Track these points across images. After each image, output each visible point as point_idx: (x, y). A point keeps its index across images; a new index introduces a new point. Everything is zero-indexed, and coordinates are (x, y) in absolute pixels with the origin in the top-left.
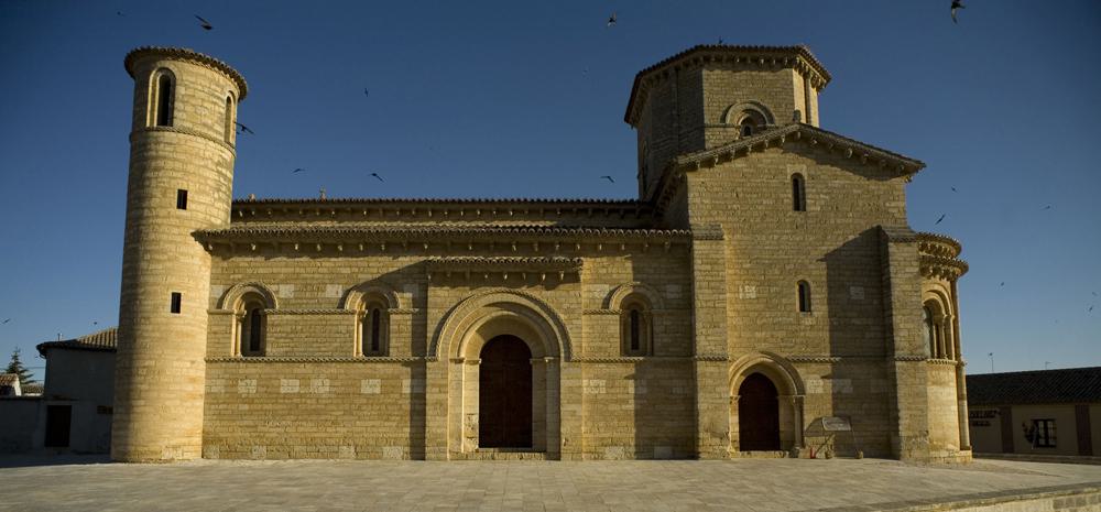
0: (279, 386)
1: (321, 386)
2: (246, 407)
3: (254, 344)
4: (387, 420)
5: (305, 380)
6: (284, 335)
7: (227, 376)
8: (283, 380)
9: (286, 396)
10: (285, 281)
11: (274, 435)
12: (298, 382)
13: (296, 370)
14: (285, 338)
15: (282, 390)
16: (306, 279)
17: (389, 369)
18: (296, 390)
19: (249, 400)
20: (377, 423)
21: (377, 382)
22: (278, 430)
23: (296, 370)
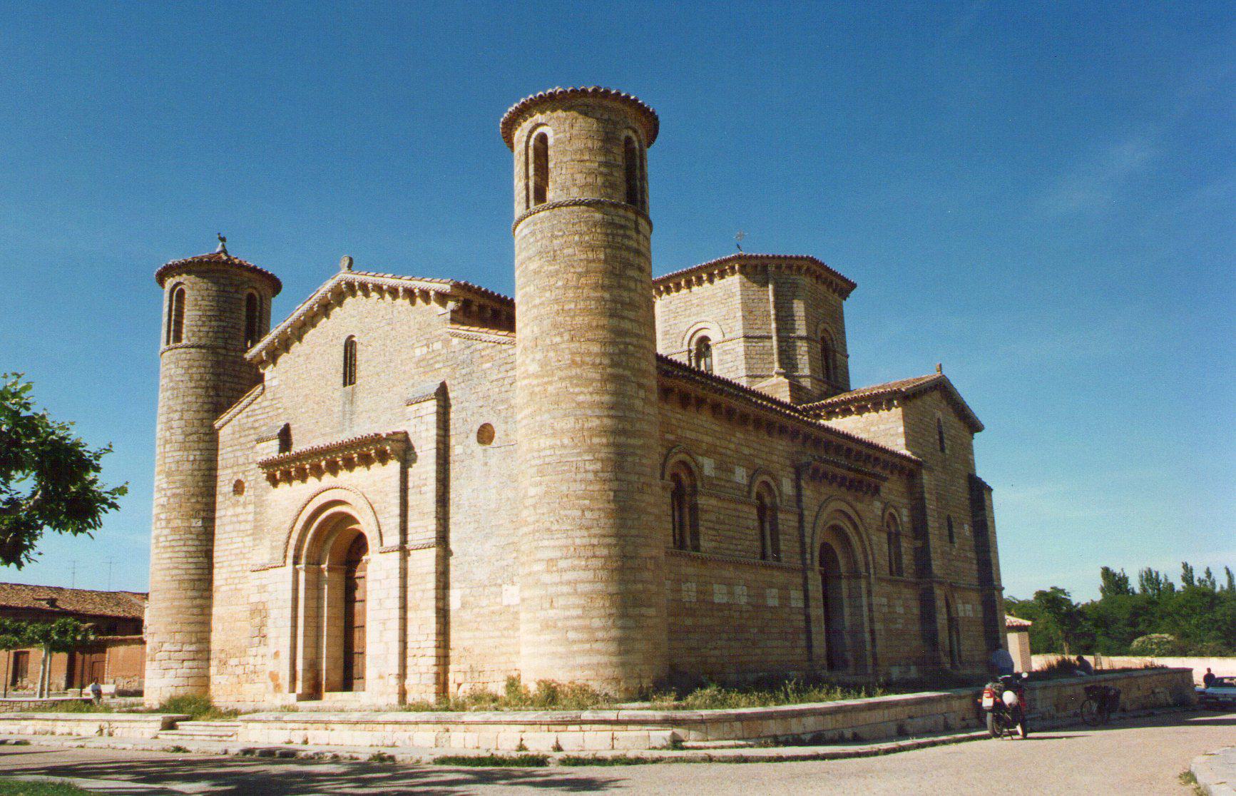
0: (712, 594)
1: (742, 596)
2: (689, 622)
3: (685, 536)
4: (786, 639)
5: (729, 584)
6: (711, 525)
7: (672, 576)
8: (716, 587)
9: (721, 607)
10: (706, 454)
11: (713, 660)
12: (724, 589)
13: (725, 573)
14: (713, 529)
15: (716, 600)
16: (721, 454)
17: (780, 577)
18: (724, 601)
19: (691, 612)
20: (780, 643)
21: (775, 591)
22: (717, 652)
23: (725, 573)
